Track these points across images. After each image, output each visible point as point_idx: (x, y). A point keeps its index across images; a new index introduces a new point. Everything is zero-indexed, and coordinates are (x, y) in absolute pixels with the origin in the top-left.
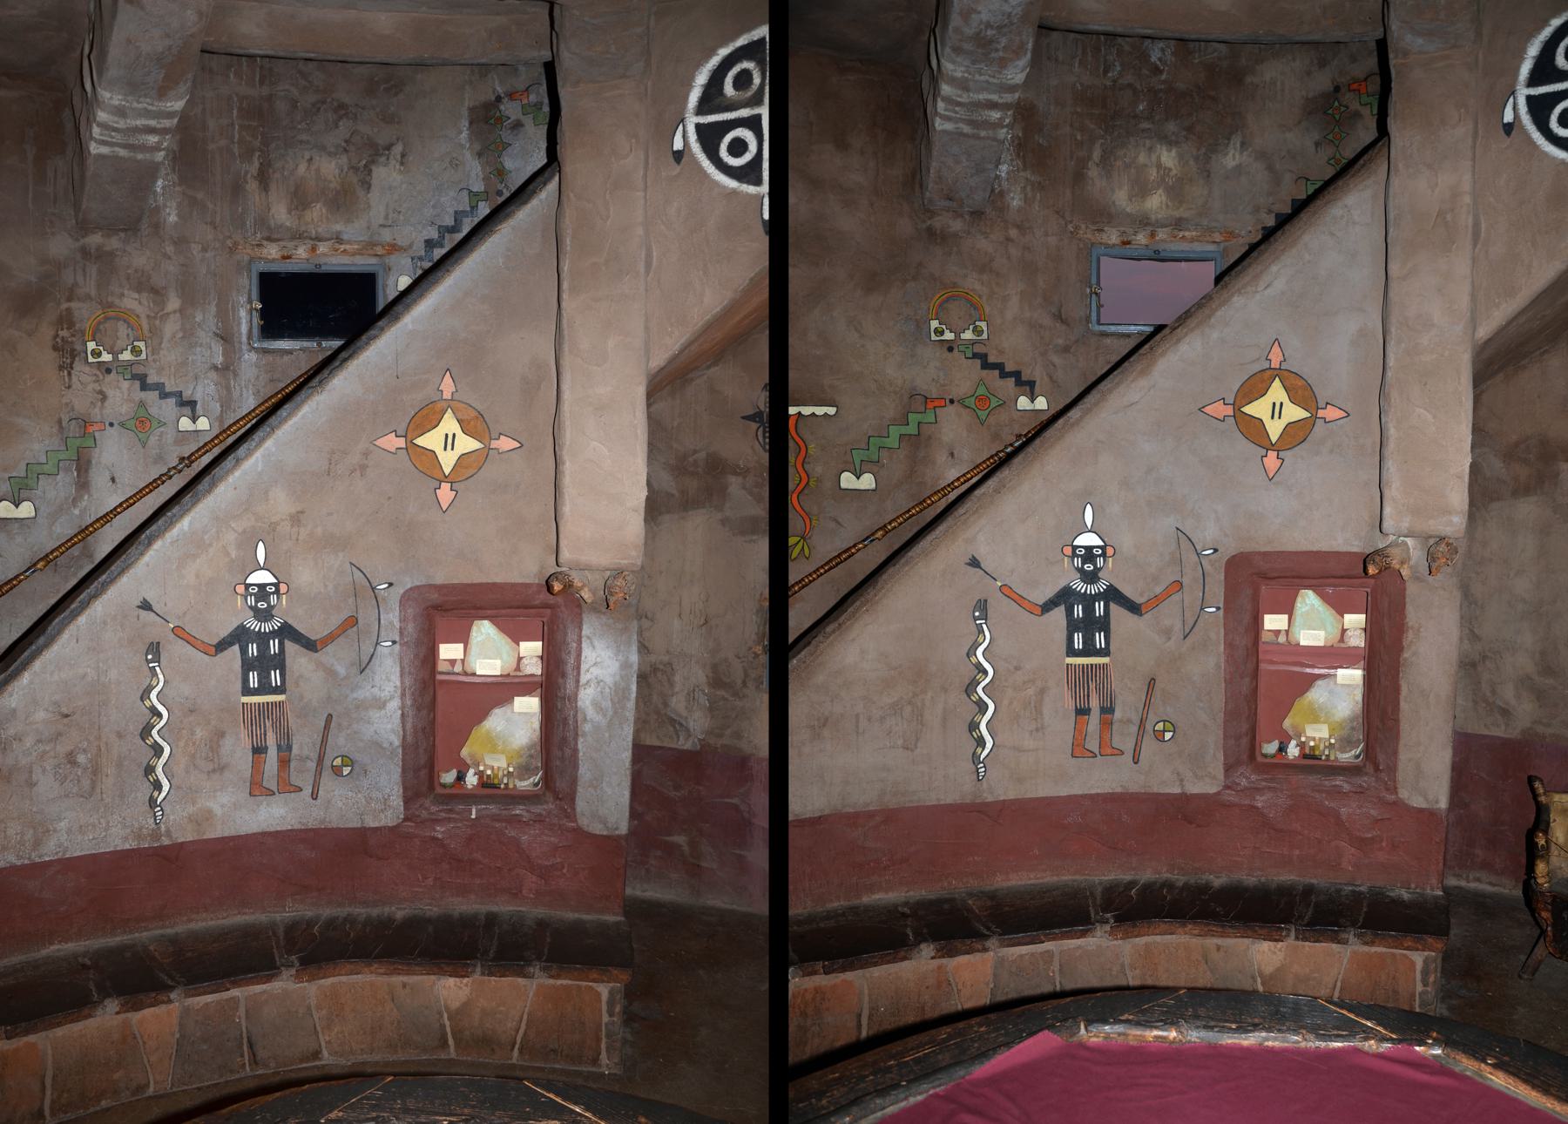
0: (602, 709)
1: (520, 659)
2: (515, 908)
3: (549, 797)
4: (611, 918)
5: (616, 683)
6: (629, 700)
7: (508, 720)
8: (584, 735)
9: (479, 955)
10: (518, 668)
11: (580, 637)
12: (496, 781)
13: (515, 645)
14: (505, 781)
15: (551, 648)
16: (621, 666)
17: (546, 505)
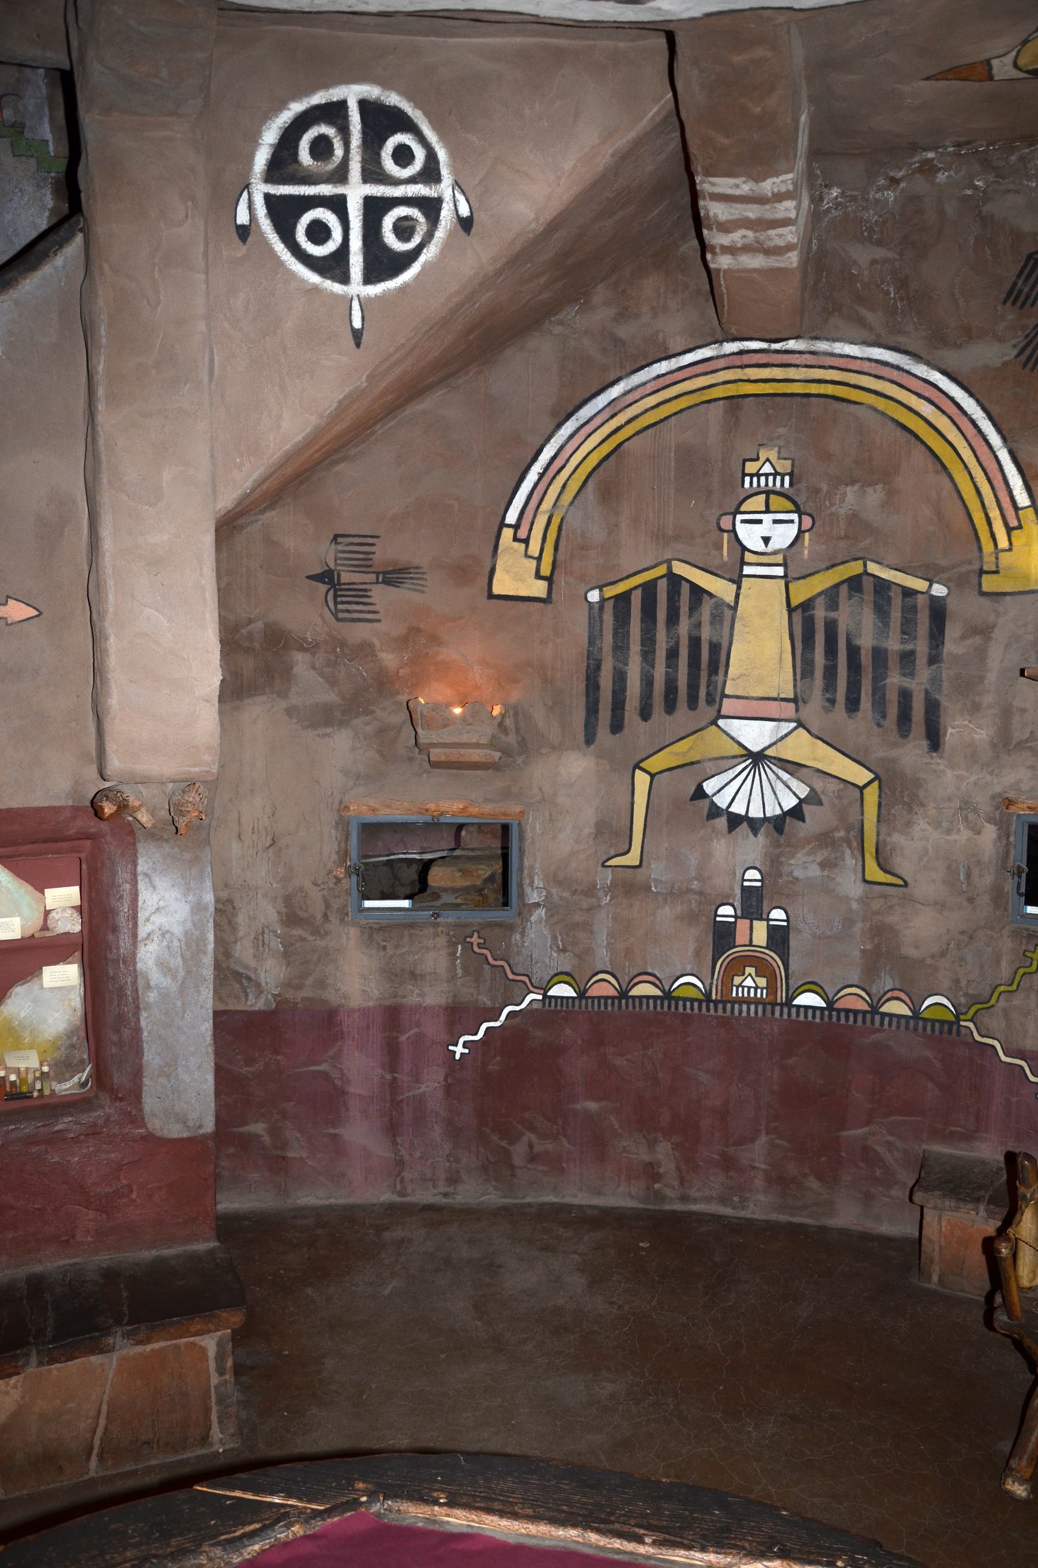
0: (170, 970)
1: (47, 913)
2: (68, 1261)
3: (105, 1099)
4: (201, 1247)
5: (186, 933)
6: (205, 953)
7: (35, 1001)
8: (148, 1007)
9: (31, 1339)
10: (45, 927)
11: (135, 875)
12: (24, 1089)
13: (38, 894)
14: (38, 1086)
15: (94, 894)
16: (192, 908)
17: (78, 696)
